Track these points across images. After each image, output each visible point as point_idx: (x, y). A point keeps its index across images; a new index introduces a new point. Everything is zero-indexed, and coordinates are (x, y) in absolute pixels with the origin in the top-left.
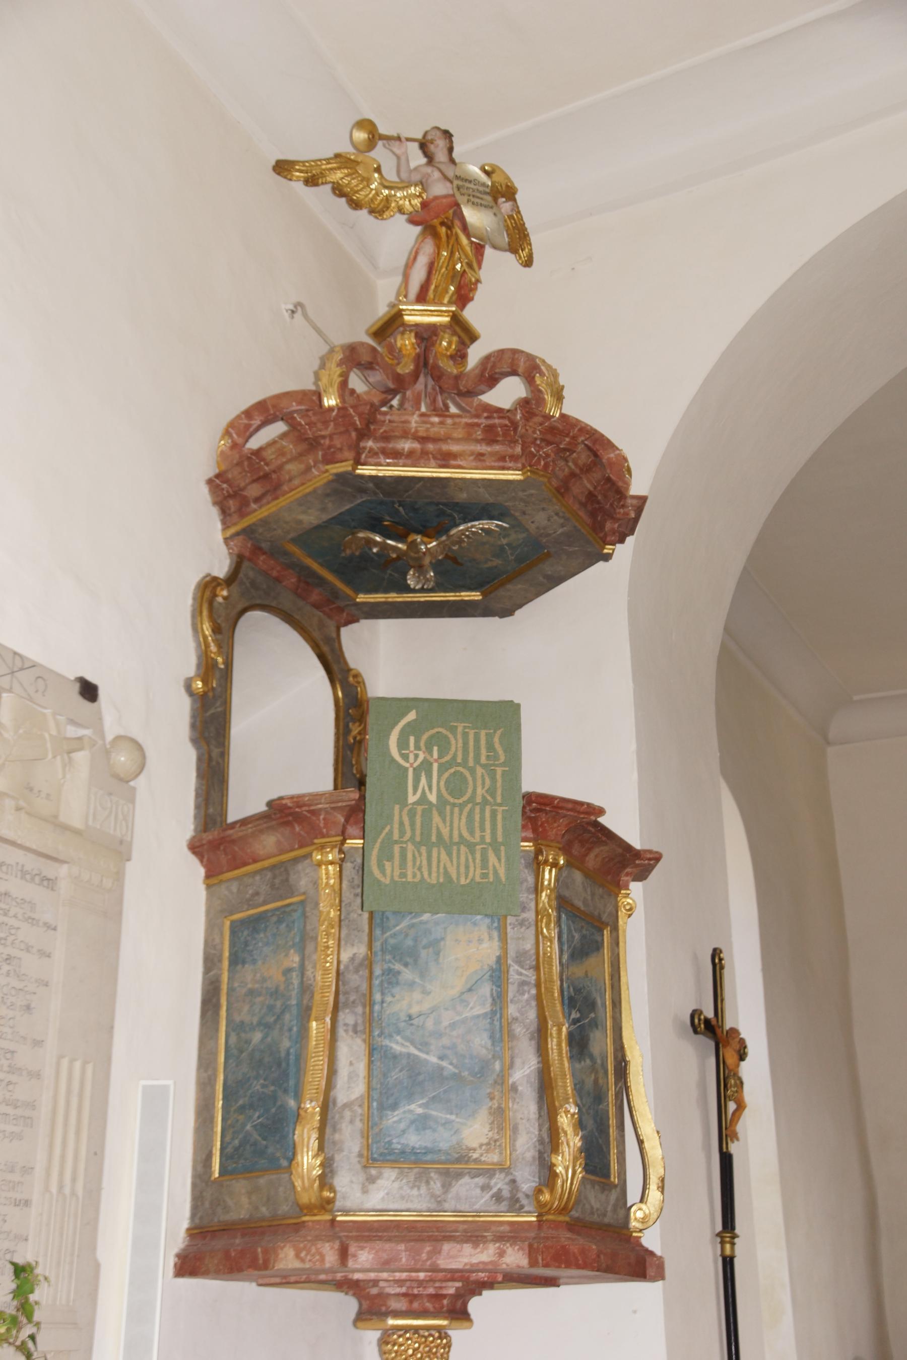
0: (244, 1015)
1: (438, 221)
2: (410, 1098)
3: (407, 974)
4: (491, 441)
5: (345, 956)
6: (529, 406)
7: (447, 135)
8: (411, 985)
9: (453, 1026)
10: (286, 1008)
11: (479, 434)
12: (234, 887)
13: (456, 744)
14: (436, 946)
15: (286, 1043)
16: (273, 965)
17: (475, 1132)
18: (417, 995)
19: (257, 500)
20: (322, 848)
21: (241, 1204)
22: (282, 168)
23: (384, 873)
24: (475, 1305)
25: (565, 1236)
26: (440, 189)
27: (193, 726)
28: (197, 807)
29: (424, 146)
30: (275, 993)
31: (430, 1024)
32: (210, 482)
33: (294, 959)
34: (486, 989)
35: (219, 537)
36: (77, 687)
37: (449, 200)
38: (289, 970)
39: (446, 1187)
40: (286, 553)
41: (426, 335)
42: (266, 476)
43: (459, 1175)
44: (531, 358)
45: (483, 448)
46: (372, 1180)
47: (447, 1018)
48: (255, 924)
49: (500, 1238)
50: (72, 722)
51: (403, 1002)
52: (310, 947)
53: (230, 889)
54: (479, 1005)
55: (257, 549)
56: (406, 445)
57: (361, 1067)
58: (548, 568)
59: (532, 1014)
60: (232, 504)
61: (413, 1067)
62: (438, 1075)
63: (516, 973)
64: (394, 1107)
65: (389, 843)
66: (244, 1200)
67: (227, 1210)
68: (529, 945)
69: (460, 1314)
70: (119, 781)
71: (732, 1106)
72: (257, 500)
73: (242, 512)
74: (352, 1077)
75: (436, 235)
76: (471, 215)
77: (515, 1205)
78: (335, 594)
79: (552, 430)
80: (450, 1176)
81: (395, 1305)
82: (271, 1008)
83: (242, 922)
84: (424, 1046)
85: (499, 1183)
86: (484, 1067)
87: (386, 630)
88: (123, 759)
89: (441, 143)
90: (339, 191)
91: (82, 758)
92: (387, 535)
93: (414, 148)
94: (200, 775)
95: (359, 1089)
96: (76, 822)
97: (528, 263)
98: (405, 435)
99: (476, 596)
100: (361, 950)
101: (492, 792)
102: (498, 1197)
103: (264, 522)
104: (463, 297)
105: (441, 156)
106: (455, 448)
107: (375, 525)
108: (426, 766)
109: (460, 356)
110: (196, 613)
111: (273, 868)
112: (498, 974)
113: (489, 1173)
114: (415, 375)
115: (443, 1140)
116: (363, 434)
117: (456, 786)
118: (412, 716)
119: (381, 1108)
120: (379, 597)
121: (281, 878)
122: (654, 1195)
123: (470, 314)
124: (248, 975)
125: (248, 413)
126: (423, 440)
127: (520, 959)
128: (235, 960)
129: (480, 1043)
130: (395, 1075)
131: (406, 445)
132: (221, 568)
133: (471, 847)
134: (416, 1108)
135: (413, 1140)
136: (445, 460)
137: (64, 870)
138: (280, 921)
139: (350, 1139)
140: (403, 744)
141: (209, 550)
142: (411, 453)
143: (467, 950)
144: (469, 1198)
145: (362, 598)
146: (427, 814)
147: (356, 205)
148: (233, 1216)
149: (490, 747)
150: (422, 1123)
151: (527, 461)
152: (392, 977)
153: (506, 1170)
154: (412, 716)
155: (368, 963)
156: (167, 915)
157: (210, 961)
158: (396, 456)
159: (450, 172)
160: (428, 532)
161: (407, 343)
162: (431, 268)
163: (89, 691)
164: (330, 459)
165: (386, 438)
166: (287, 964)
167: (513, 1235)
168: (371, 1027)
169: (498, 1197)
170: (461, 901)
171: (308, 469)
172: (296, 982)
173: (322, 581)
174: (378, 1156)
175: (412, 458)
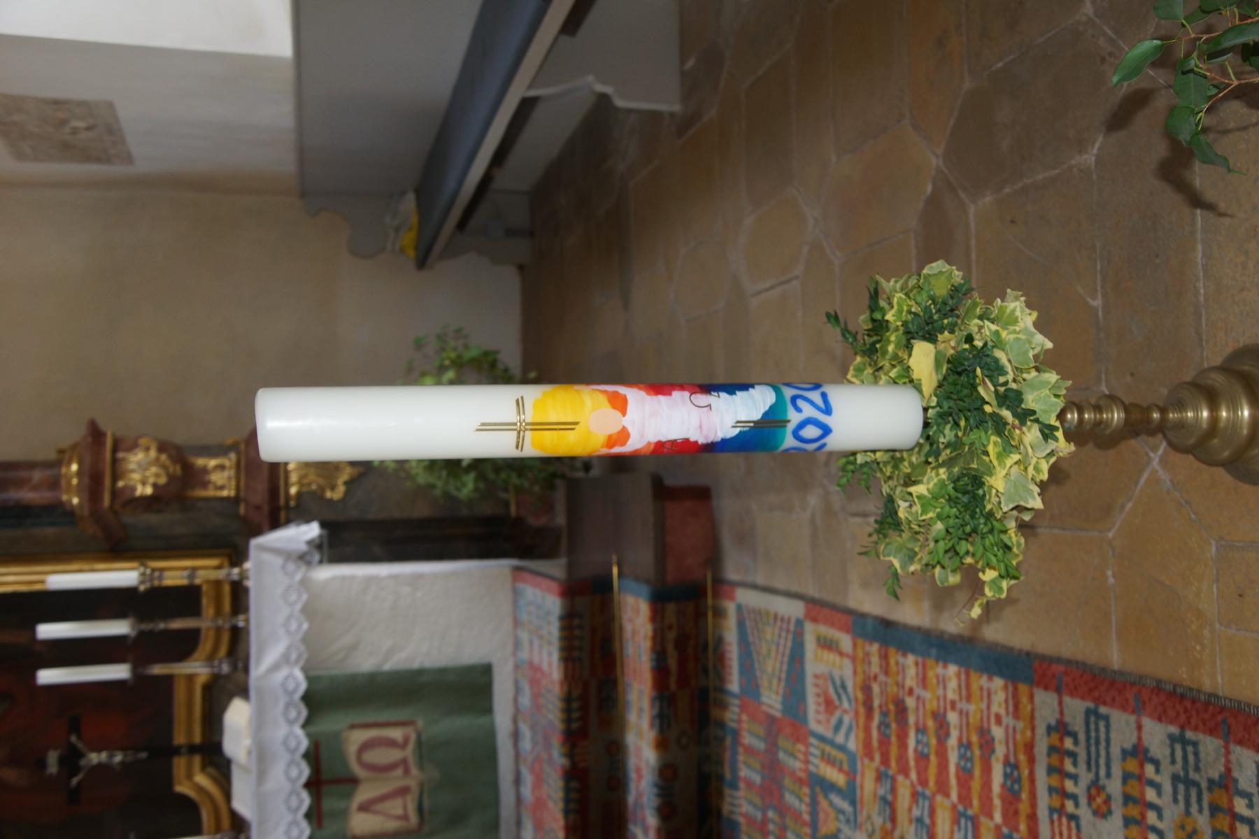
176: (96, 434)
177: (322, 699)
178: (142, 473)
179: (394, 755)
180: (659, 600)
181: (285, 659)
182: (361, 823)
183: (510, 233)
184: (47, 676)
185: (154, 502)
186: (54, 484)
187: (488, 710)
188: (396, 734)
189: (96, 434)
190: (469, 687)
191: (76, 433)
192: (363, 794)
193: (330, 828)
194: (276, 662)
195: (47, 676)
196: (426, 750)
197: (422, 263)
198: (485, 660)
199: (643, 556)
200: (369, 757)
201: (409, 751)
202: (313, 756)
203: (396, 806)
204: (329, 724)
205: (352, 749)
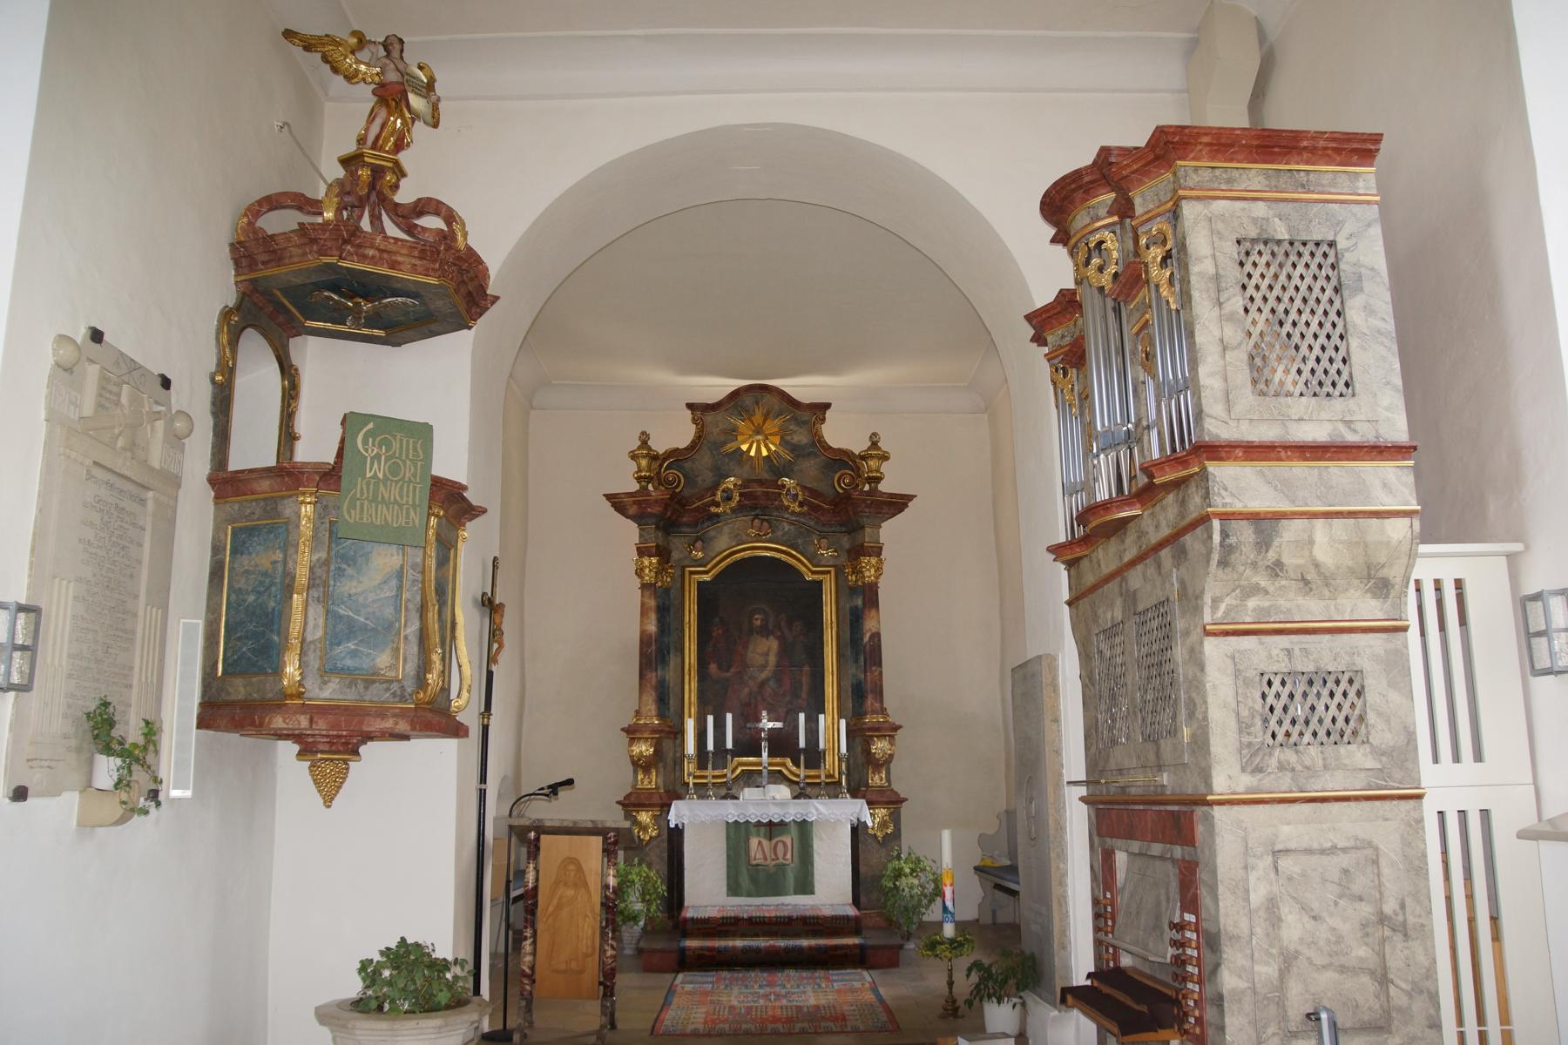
0: (241, 584)
1: (391, 97)
2: (348, 640)
3: (350, 571)
4: (421, 258)
5: (315, 558)
6: (447, 237)
7: (401, 42)
8: (352, 577)
9: (374, 601)
10: (272, 584)
11: (416, 253)
12: (236, 507)
13: (396, 445)
14: (367, 557)
15: (272, 604)
16: (263, 558)
17: (383, 660)
18: (354, 583)
19: (264, 263)
20: (304, 494)
21: (239, 689)
22: (289, 34)
23: (350, 516)
24: (362, 749)
25: (429, 715)
26: (392, 76)
27: (213, 404)
28: (213, 454)
29: (386, 45)
30: (265, 574)
31: (361, 599)
32: (232, 245)
33: (279, 556)
34: (394, 583)
35: (232, 280)
36: (159, 380)
37: (398, 87)
38: (276, 562)
39: (366, 688)
40: (273, 295)
41: (378, 172)
42: (274, 251)
43: (374, 682)
44: (450, 210)
45: (418, 262)
46: (325, 683)
47: (371, 597)
48: (252, 531)
49: (395, 716)
50: (157, 403)
51: (348, 587)
52: (291, 550)
53: (233, 507)
54: (389, 592)
55: (255, 290)
56: (371, 252)
57: (321, 621)
58: (433, 327)
59: (418, 598)
60: (244, 262)
61: (351, 624)
62: (364, 628)
63: (410, 574)
64: (339, 644)
65: (354, 499)
66: (242, 689)
67: (229, 694)
68: (419, 560)
69: (356, 753)
70: (176, 441)
71: (496, 646)
72: (264, 263)
73: (252, 266)
74: (316, 626)
75: (388, 106)
76: (412, 98)
77: (403, 699)
78: (292, 318)
79: (459, 258)
80: (369, 683)
81: (321, 747)
82: (261, 583)
83: (241, 529)
84: (357, 612)
85: (395, 687)
86: (390, 625)
87: (312, 342)
88: (179, 425)
89: (398, 47)
90: (325, 59)
91: (160, 424)
92: (341, 295)
93: (381, 48)
94: (215, 435)
95: (319, 633)
96: (156, 464)
97: (436, 126)
98: (372, 247)
99: (381, 333)
100: (324, 555)
101: (414, 475)
102: (394, 694)
103: (266, 278)
104: (400, 146)
105: (396, 54)
106: (400, 259)
107: (335, 288)
108: (378, 457)
109: (396, 187)
110: (219, 331)
111: (265, 499)
112: (400, 574)
113: (390, 682)
114: (368, 195)
115: (365, 664)
116: (345, 242)
117: (394, 470)
118: (371, 426)
119: (331, 644)
120: (321, 324)
121: (271, 507)
122: (465, 694)
123: (403, 157)
124: (245, 562)
125: (260, 202)
126: (381, 251)
127: (414, 567)
128: (234, 552)
129: (389, 612)
130: (340, 627)
131: (371, 252)
132: (232, 302)
133: (401, 506)
134: (351, 646)
135: (349, 662)
136: (394, 265)
137: (150, 494)
138: (270, 532)
139: (314, 661)
140: (365, 442)
141: (222, 289)
142: (373, 257)
143: (385, 560)
144: (377, 694)
145: (309, 323)
146: (376, 485)
147: (335, 70)
148: (233, 697)
149: (415, 450)
150: (354, 654)
151: (442, 274)
152: (340, 572)
153: (399, 681)
154: (371, 426)
155: (327, 563)
156: (196, 520)
157: (217, 549)
158: (363, 258)
159: (401, 67)
160: (366, 297)
161: (364, 173)
162: (383, 126)
163: (166, 383)
164: (322, 253)
165: (359, 246)
166: (274, 558)
167: (403, 714)
168: (327, 600)
169: (394, 694)
170: (397, 538)
171: (305, 254)
172: (280, 569)
173: (288, 311)
174: (329, 671)
175: (372, 260)
176: (896, 728)
177: (804, 827)
178: (879, 747)
179: (780, 854)
180: (861, 947)
181: (820, 813)
182: (754, 842)
183: (994, 912)
184: (802, 716)
185: (868, 752)
186: (874, 712)
187: (796, 893)
188: (789, 856)
189: (896, 728)
190: (805, 885)
191: (894, 718)
192: (765, 843)
193: (753, 830)
194: (818, 809)
195: (802, 716)
196: (781, 868)
197: (977, 869)
198: (816, 889)
199: (870, 942)
200: (780, 846)
201: (781, 861)
202: (782, 824)
203: (760, 855)
204: (794, 830)
205: (783, 838)
